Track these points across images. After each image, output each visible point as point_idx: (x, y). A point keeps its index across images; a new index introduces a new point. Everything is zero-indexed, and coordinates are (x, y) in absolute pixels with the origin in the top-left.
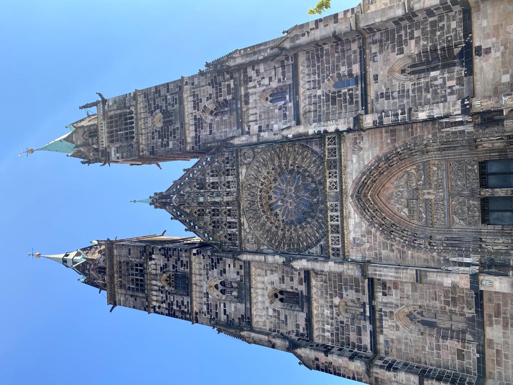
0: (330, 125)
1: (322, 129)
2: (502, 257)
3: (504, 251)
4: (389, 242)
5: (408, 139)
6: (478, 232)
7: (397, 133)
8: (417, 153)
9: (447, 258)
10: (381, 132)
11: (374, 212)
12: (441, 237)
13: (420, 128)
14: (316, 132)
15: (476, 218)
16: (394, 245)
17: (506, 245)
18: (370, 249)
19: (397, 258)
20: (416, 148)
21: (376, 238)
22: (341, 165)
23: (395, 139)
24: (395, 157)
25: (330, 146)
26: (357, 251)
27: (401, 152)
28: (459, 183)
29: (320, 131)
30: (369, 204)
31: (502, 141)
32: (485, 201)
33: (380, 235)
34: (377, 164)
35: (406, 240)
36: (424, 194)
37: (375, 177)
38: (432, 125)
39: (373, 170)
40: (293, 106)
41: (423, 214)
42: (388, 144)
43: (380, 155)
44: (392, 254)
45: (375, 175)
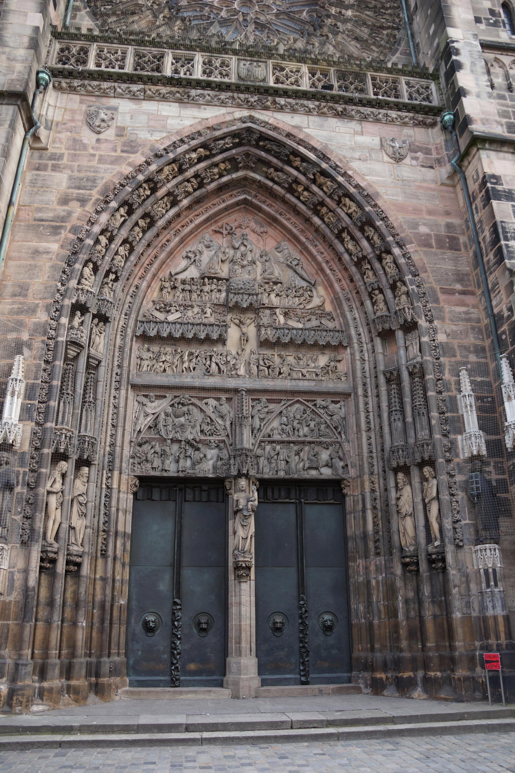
0: (477, 79)
1: (463, 58)
2: (18, 518)
3: (39, 525)
4: (95, 194)
5: (431, 279)
6: (111, 462)
7: (449, 254)
8: (382, 305)
9: (26, 350)
10: (448, 213)
11: (196, 176)
12: (101, 348)
13: (466, 313)
14: (455, 45)
15: (157, 463)
16: (83, 206)
17: (62, 535)
18: (77, 145)
19: (39, 210)
20: (404, 297)
21: (112, 163)
22: (350, 101)
23: (430, 246)
24: (372, 246)
25: (405, 87)
26: (73, 112)
27: (388, 259)
28: (276, 424)
29: (457, 53)
30: (222, 166)
31: (422, 540)
32: (214, 490)
33: (120, 173)
34: (352, 190)
35: (97, 242)
36: (240, 324)
37: (307, 189)
38: (476, 346)
39: (333, 180)
40: (500, 40)
41: (178, 315)
42: (415, 225)
43: (380, 203)
44: (53, 197)
45: (315, 188)
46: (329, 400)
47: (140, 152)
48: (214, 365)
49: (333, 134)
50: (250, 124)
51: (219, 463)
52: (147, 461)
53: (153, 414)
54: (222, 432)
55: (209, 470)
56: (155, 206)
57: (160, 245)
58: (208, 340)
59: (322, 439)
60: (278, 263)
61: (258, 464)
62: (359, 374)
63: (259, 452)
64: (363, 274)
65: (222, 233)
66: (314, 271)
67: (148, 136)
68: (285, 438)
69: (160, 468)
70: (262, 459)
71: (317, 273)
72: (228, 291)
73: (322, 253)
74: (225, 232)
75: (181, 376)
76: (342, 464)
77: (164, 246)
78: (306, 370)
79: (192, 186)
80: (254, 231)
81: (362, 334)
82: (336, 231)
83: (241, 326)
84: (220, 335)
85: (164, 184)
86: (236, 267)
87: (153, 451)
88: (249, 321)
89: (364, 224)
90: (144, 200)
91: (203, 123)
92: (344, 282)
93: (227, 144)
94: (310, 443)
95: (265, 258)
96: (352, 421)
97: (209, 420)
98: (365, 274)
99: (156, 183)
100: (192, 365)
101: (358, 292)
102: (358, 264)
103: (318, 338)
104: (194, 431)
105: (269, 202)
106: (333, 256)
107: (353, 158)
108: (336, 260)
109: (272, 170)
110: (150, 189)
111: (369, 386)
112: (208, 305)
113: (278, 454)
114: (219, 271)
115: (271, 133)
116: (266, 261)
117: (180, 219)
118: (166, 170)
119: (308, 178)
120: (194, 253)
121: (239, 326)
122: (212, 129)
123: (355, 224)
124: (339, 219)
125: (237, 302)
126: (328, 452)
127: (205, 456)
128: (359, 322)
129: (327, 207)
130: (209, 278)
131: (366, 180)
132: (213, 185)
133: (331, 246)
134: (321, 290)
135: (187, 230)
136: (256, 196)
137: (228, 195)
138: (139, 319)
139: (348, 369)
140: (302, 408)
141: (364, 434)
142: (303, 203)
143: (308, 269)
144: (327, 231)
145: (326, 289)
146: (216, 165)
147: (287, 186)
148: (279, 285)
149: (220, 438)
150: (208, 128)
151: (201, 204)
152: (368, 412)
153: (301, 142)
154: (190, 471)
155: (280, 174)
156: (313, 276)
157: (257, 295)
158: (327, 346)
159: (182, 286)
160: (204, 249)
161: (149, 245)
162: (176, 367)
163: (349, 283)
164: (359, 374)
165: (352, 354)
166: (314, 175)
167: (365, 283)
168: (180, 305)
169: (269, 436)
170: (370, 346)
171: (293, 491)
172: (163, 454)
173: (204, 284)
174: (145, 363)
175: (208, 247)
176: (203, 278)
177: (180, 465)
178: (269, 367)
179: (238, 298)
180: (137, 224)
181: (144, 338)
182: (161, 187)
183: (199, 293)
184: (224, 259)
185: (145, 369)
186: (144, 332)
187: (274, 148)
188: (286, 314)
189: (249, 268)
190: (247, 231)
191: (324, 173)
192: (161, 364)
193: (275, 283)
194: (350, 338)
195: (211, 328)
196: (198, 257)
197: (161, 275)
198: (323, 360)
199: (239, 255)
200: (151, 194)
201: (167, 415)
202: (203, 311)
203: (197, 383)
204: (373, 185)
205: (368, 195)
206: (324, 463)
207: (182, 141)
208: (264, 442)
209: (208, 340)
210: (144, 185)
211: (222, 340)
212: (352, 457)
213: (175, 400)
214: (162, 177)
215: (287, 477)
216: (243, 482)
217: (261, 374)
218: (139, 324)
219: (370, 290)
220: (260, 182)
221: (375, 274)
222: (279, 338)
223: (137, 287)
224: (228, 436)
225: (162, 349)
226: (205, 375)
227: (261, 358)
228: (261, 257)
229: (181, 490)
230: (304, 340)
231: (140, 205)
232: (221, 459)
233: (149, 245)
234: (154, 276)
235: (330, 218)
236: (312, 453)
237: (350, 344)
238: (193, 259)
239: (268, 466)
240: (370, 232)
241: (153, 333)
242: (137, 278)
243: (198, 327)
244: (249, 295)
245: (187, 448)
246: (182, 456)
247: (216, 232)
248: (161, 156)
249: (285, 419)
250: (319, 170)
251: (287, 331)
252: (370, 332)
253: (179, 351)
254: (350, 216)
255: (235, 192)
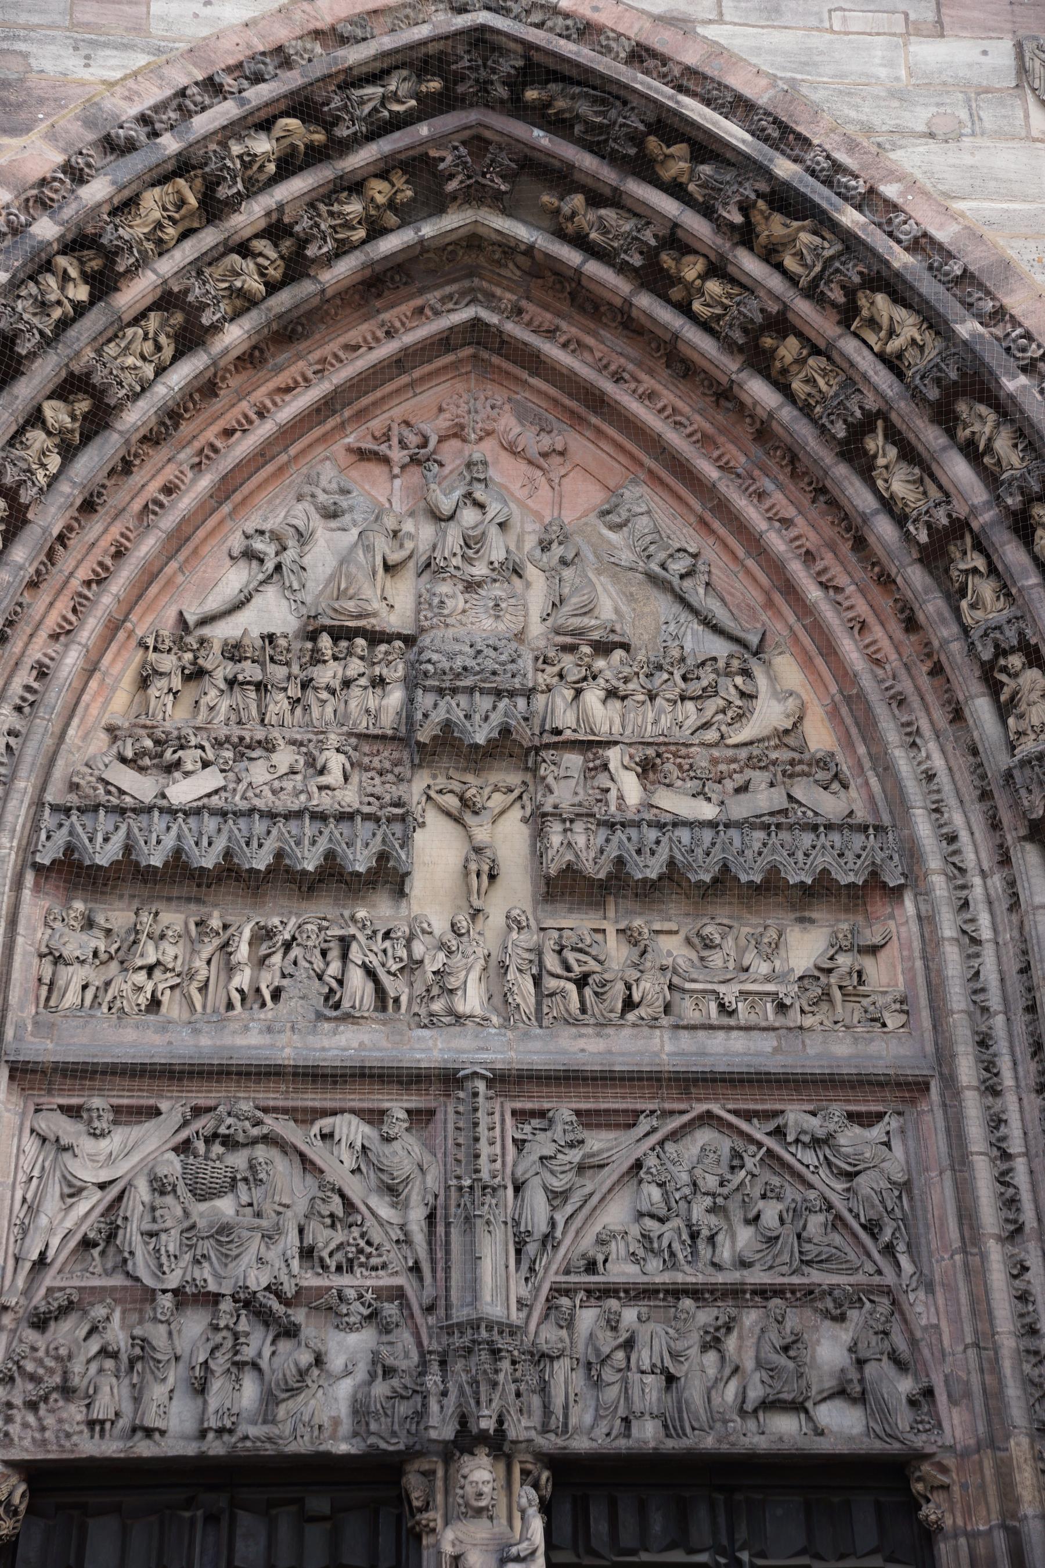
11: (276, 229)
15: (111, 1397)
24: (991, 478)
28: (616, 1215)
34: (901, 259)
37: (717, 269)
39: (824, 223)
41: (209, 780)
43: (1016, 302)
45: (750, 264)
46: (838, 1109)
47: (43, 127)
48: (356, 978)
49: (818, 41)
50: (484, 17)
51: (381, 1389)
52: (67, 1391)
53: (102, 1186)
54: (393, 1256)
55: (336, 1422)
56: (111, 349)
57: (137, 506)
58: (333, 878)
59: (816, 1276)
60: (614, 568)
61: (544, 1389)
62: (957, 998)
63: (550, 1336)
64: (955, 594)
65: (386, 460)
66: (756, 597)
67: (72, 64)
68: (655, 1273)
69: (123, 1423)
70: (561, 1369)
71: (770, 604)
72: (412, 684)
73: (787, 523)
74: (398, 455)
75: (221, 1023)
76: (906, 1385)
77: (151, 509)
78: (735, 988)
79: (261, 271)
80: (512, 450)
81: (964, 836)
82: (840, 430)
83: (469, 818)
84: (383, 857)
85: (142, 263)
86: (444, 588)
87: (94, 1347)
88: (498, 800)
89: (952, 393)
90: (64, 324)
91: (298, 16)
92: (878, 632)
93: (396, 98)
94: (764, 1293)
95: (557, 551)
96: (940, 1195)
97: (336, 1205)
98: (963, 592)
99: (110, 255)
100: (267, 980)
101: (938, 670)
102: (934, 555)
103: (781, 857)
104: (273, 1255)
105: (570, 330)
106: (829, 532)
107: (900, 132)
108: (845, 548)
109: (578, 200)
110: (87, 277)
111: (1002, 1046)
112: (333, 740)
113: (629, 1345)
114: (376, 605)
115: (567, 48)
116: (564, 562)
117: (217, 405)
118: (152, 202)
119: (721, 225)
120: (276, 537)
121: (458, 820)
122: (334, 36)
123: (916, 395)
124: (852, 381)
125: (448, 725)
126: (845, 1335)
127: (319, 1361)
128: (947, 788)
129: (800, 335)
130: (338, 634)
131: (955, 217)
132: (345, 268)
133: (822, 492)
134: (788, 670)
135: (244, 446)
136: (519, 311)
137: (407, 308)
138: (49, 798)
139: (911, 982)
140: (725, 1144)
141: (995, 1254)
142: (706, 326)
143: (734, 589)
144: (805, 432)
145: (806, 663)
146: (355, 186)
147: (637, 260)
148: (618, 654)
149: (384, 1280)
150: (317, 34)
151: (302, 346)
152: (1006, 1156)
153: (689, 80)
154: (253, 1431)
155: (608, 214)
156: (754, 617)
157: (529, 693)
158: (819, 893)
159: (230, 669)
160: (317, 522)
161: (88, 507)
162: (204, 988)
163: (899, 634)
164: (957, 998)
165: (926, 921)
166: (745, 208)
167: (965, 630)
168: (218, 744)
169: (591, 1267)
170: (996, 881)
171: (702, 1514)
172: (140, 1358)
173: (316, 659)
174: (74, 976)
175: (331, 514)
176: (313, 636)
177: (213, 1403)
178: (581, 982)
179: (454, 708)
180: (35, 418)
181: (72, 874)
182: (131, 272)
183: (294, 691)
184: (394, 558)
185: (72, 998)
186: (70, 849)
187: (584, 108)
188: (646, 769)
189: (497, 590)
190: (487, 449)
191: (786, 200)
192: (141, 977)
193: (603, 648)
194: (912, 853)
195: (345, 827)
196: (290, 555)
197: (142, 625)
198: (805, 948)
199: (453, 538)
200: (95, 298)
201: (160, 1187)
202: (311, 761)
203: (288, 1049)
204: (988, 233)
205: (967, 277)
206: (830, 1384)
207: (212, 86)
208: (567, 1292)
209: (333, 878)
210: (62, 261)
211: (389, 877)
212: (952, 1360)
213: (197, 1125)
214: (136, 229)
215: (670, 1444)
216: (480, 1473)
217: (553, 1008)
218: (48, 819)
219: (987, 655)
220: (530, 250)
221: (1005, 591)
222: (620, 861)
223: (42, 672)
224: (416, 1269)
225: (146, 918)
226: (320, 1016)
227: (550, 945)
228: (545, 546)
229: (212, 1518)
230: (725, 868)
231: (48, 342)
232: (389, 1372)
233: (88, 507)
234: (113, 627)
235: (814, 378)
236: (773, 1336)
237: (914, 878)
238: (270, 563)
239: (589, 1394)
240: (980, 422)
241: (106, 854)
242: (43, 635)
243: (293, 826)
244: (498, 693)
245: (243, 1326)
246: (221, 1362)
247: (363, 455)
248: (130, 147)
249: (656, 1193)
250: (763, 187)
251: (652, 834)
252: (995, 825)
253: (215, 923)
254: (893, 363)
255: (432, 297)
